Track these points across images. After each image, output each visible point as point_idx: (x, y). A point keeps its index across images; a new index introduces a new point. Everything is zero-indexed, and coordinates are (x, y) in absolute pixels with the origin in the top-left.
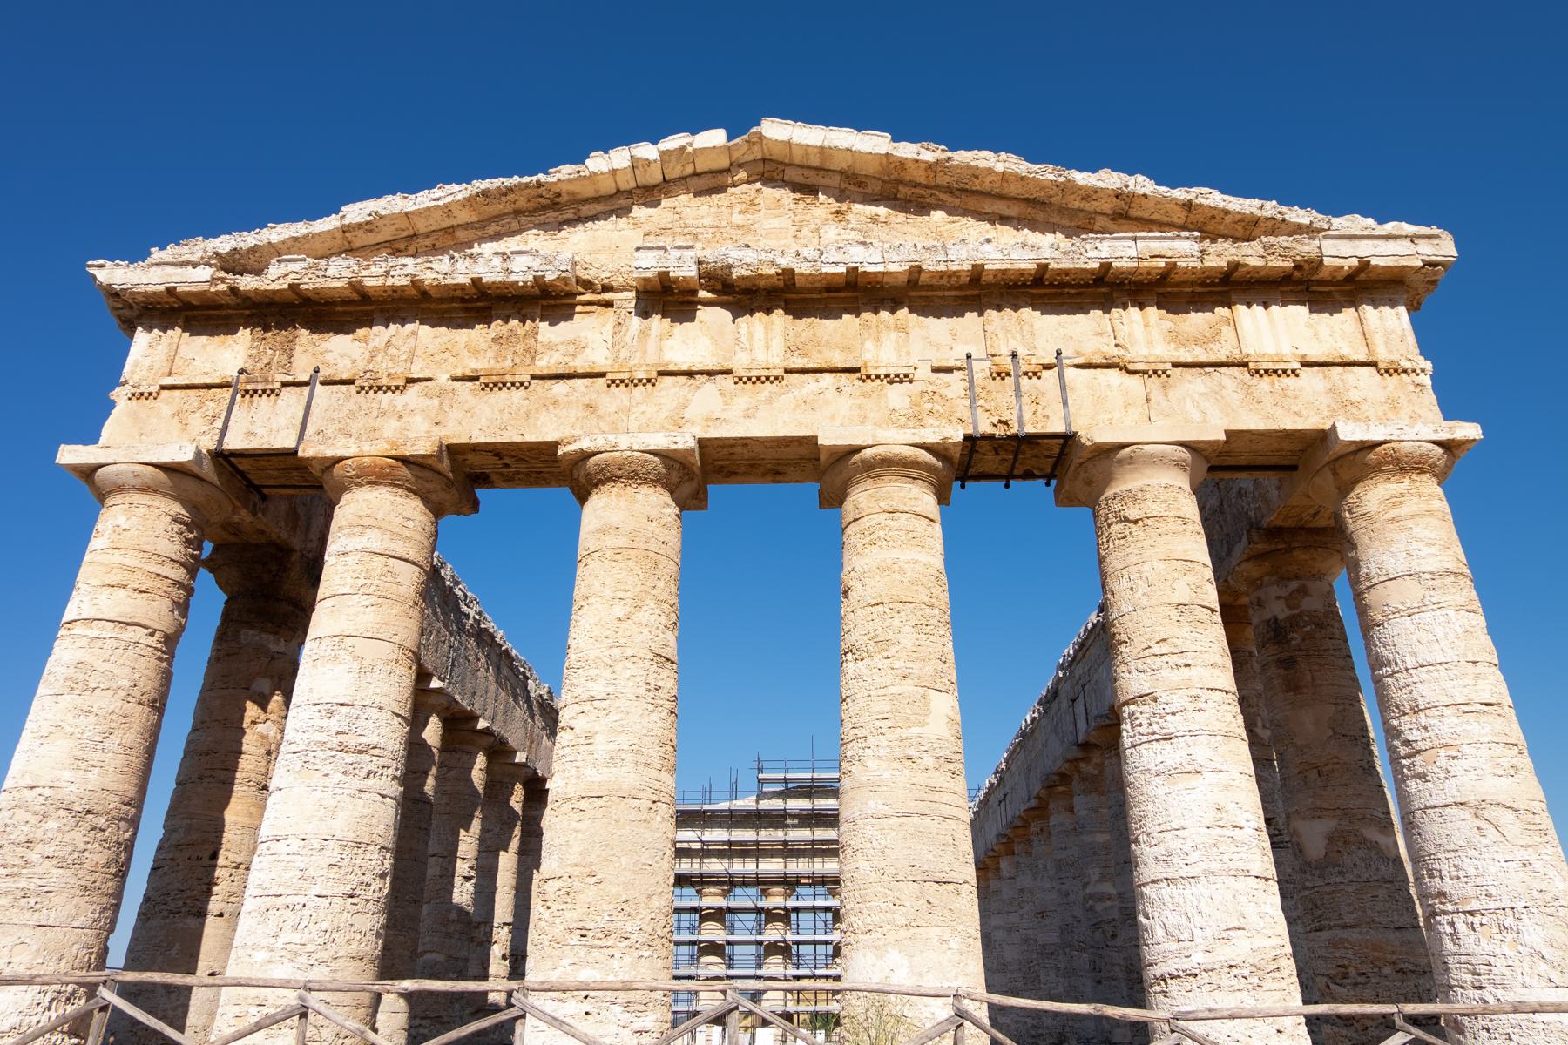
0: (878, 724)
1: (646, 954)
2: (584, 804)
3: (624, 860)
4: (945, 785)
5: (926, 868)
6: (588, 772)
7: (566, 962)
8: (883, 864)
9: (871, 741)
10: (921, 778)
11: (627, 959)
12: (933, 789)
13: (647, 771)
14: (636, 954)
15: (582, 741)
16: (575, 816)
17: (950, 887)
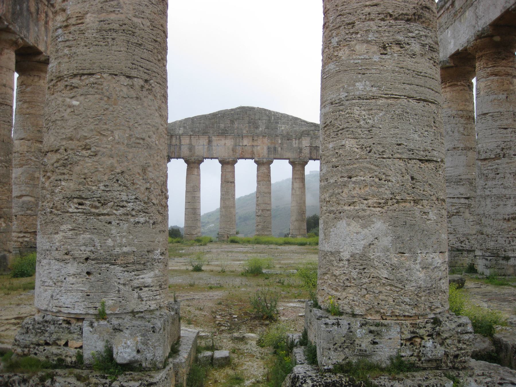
0: (367, 10)
1: (142, 220)
2: (75, 81)
3: (117, 134)
4: (429, 71)
5: (412, 147)
6: (80, 50)
7: (64, 227)
8: (371, 142)
9: (359, 25)
10: (409, 62)
11: (125, 226)
12: (419, 74)
13: (137, 50)
14: (132, 220)
15: (72, 21)
16: (67, 93)
17: (431, 165)
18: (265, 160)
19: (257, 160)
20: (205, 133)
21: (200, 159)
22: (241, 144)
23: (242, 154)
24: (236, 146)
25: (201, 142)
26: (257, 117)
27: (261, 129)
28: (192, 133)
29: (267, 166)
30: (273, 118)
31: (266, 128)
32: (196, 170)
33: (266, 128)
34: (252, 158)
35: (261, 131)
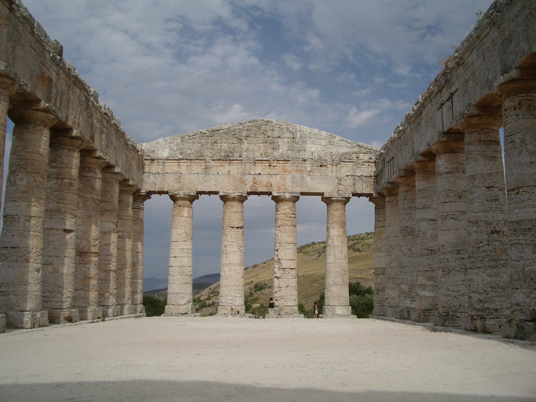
18: (287, 195)
19: (275, 194)
20: (200, 158)
21: (192, 194)
22: (252, 173)
23: (253, 186)
24: (245, 175)
25: (194, 169)
26: (276, 134)
27: (281, 151)
28: (181, 157)
29: (290, 204)
30: (298, 136)
31: (289, 150)
32: (186, 209)
33: (289, 150)
34: (269, 194)
35: (282, 154)
